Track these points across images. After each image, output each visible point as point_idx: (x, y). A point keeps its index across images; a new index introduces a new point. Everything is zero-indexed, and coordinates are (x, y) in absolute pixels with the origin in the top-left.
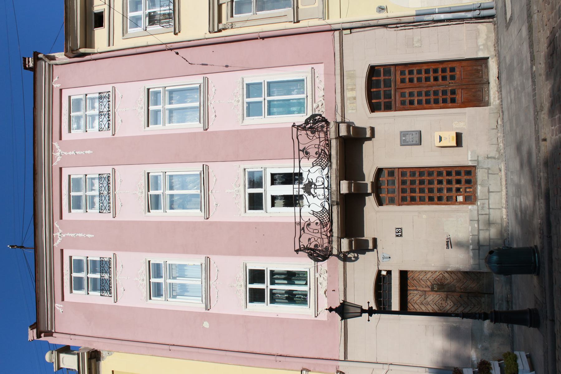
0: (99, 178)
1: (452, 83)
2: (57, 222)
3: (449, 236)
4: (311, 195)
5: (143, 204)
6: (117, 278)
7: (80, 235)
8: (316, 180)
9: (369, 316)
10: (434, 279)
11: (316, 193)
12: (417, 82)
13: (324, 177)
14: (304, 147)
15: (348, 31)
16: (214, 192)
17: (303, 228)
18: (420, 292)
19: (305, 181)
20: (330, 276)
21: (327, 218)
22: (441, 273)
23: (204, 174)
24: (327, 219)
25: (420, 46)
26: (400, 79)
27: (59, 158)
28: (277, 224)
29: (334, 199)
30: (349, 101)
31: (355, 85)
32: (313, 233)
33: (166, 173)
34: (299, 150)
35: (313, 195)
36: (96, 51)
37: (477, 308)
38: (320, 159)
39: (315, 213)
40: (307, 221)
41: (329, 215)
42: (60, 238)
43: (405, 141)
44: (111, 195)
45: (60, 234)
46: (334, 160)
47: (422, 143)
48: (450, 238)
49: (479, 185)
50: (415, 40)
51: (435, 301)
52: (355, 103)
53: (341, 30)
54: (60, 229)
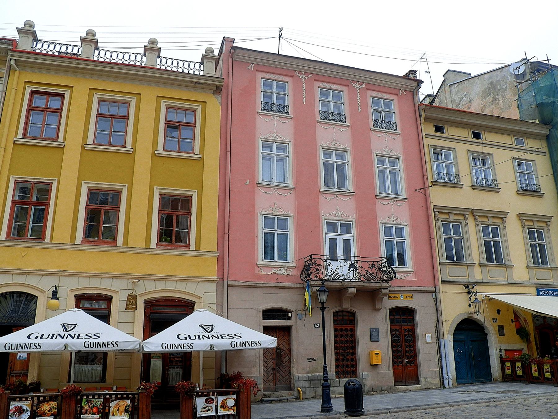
5: (327, 145)
7: (304, 93)
22: (288, 355)
27: (355, 86)
33: (347, 164)
34: (373, 261)
36: (422, 125)
37: (266, 380)
41: (337, 279)
44: (331, 122)
46: (367, 284)
47: (372, 342)
53: (435, 292)
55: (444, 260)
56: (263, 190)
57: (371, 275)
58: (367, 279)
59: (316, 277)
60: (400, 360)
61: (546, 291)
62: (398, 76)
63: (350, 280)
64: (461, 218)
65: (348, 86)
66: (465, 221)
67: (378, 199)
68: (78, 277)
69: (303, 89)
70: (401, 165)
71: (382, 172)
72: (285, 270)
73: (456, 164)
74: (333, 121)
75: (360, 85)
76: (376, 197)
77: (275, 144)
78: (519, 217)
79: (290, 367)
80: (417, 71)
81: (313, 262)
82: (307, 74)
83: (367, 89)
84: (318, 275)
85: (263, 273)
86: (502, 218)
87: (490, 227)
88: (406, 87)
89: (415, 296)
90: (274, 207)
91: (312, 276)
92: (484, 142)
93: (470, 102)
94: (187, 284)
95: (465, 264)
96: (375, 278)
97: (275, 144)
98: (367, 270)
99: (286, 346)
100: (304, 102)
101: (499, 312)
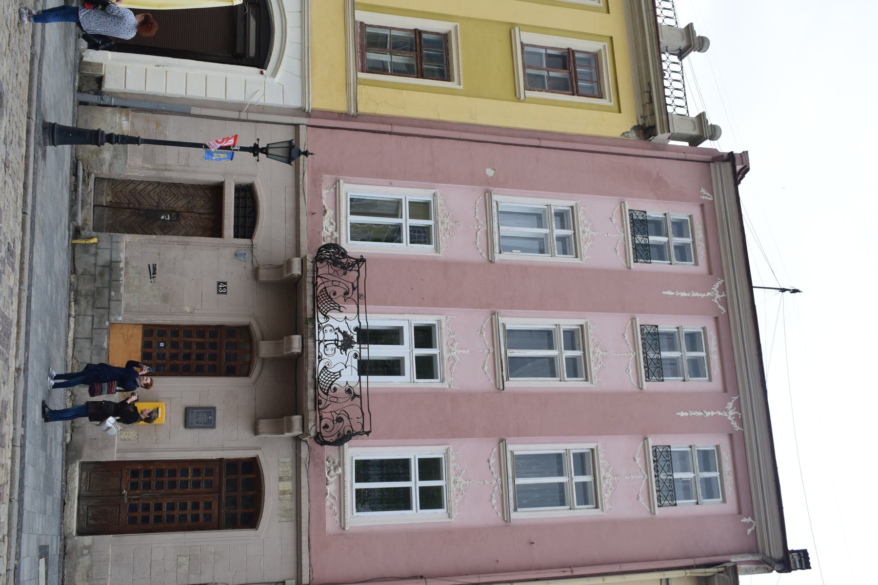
0: (663, 376)
1: (134, 500)
2: (723, 313)
3: (151, 281)
4: (342, 332)
6: (622, 234)
7: (684, 294)
8: (335, 352)
9: (258, 145)
10: (175, 227)
12: (186, 503)
13: (324, 356)
14: (354, 400)
16: (486, 351)
17: (354, 289)
18: (196, 211)
19: (351, 352)
20: (319, 233)
21: (320, 301)
23: (503, 376)
24: (320, 299)
25: (178, 558)
26: (213, 508)
27: (730, 407)
28: (394, 304)
30: (290, 475)
31: (280, 499)
32: (339, 282)
34: (360, 396)
35: (340, 331)
37: (117, 189)
38: (330, 381)
39: (338, 308)
40: (349, 298)
42: (715, 290)
43: (209, 414)
45: (715, 296)
46: (310, 379)
47: (183, 410)
48: (151, 279)
49: (104, 349)
50: (185, 568)
51: (174, 199)
52: (280, 473)
54: (717, 304)
56: (480, 200)
57: (330, 383)
58: (322, 375)
63: (317, 339)
68: (301, 60)
80: (810, 568)
82: (724, 302)
85: (325, 192)
90: (450, 221)
94: (297, 75)
96: (324, 392)
100: (667, 293)
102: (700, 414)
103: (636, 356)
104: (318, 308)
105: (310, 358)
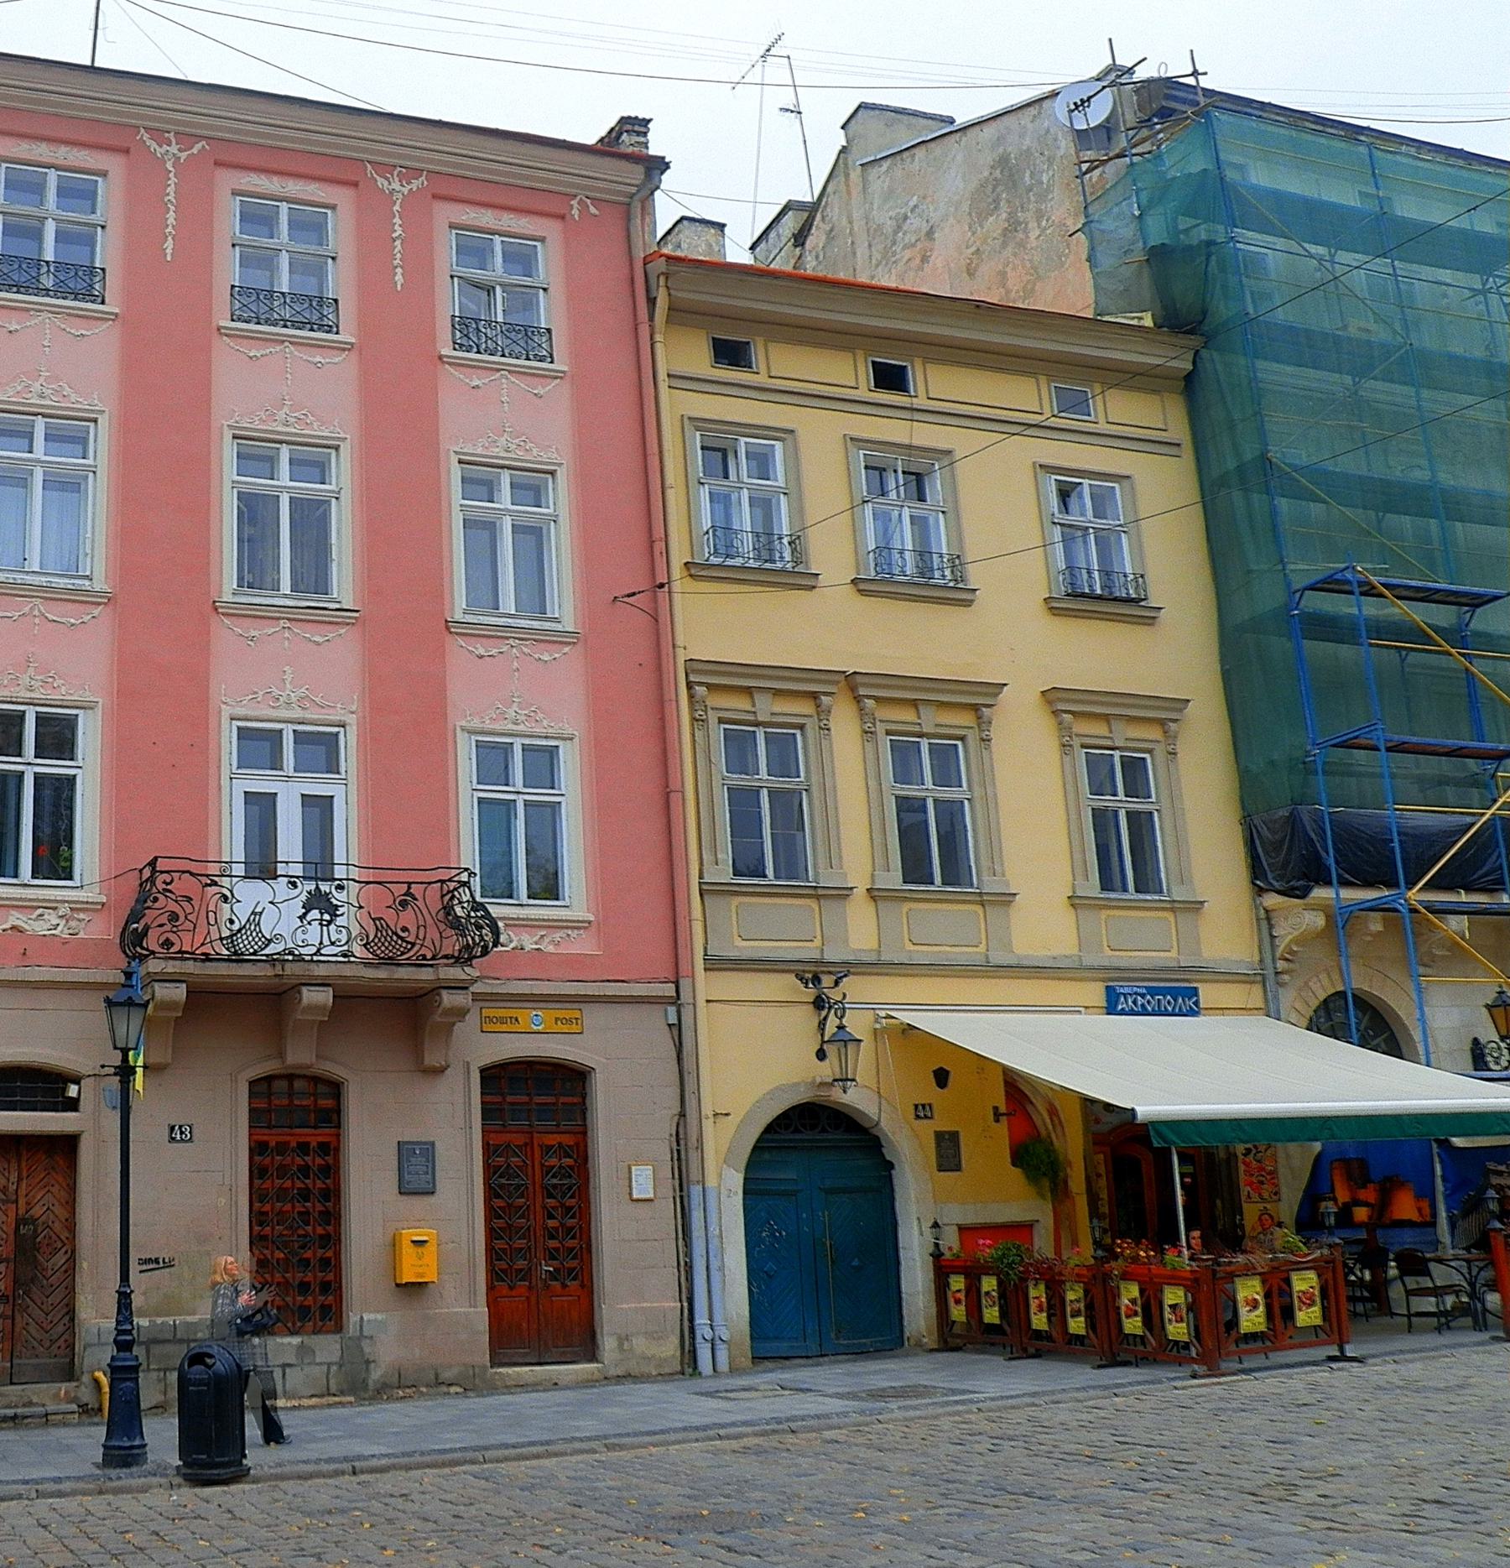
5: (256, 424)
11: (309, 923)
15: (673, 1020)
16: (287, 635)
17: (215, 884)
27: (386, 183)
29: (289, 969)
34: (409, 884)
35: (305, 914)
36: (658, 337)
41: (255, 953)
46: (382, 973)
53: (676, 1000)
55: (723, 873)
57: (395, 938)
59: (168, 944)
60: (521, 1264)
61: (1143, 996)
62: (564, 141)
64: (806, 708)
65: (355, 185)
66: (820, 720)
67: (457, 634)
69: (166, 199)
70: (561, 498)
71: (481, 529)
72: (62, 917)
73: (794, 492)
74: (285, 326)
75: (405, 178)
76: (448, 628)
77: (40, 423)
78: (1050, 703)
79: (71, 1291)
81: (161, 886)
82: (186, 138)
83: (434, 196)
84: (173, 937)
86: (975, 708)
87: (924, 744)
88: (601, 184)
89: (594, 1017)
91: (152, 942)
92: (921, 402)
93: (930, 234)
95: (811, 892)
96: (409, 950)
97: (40, 423)
98: (380, 919)
99: (58, 1210)
100: (169, 251)
101: (941, 1077)
102: (398, 243)
103: (291, 343)
104: (255, 953)
105: (347, 971)
